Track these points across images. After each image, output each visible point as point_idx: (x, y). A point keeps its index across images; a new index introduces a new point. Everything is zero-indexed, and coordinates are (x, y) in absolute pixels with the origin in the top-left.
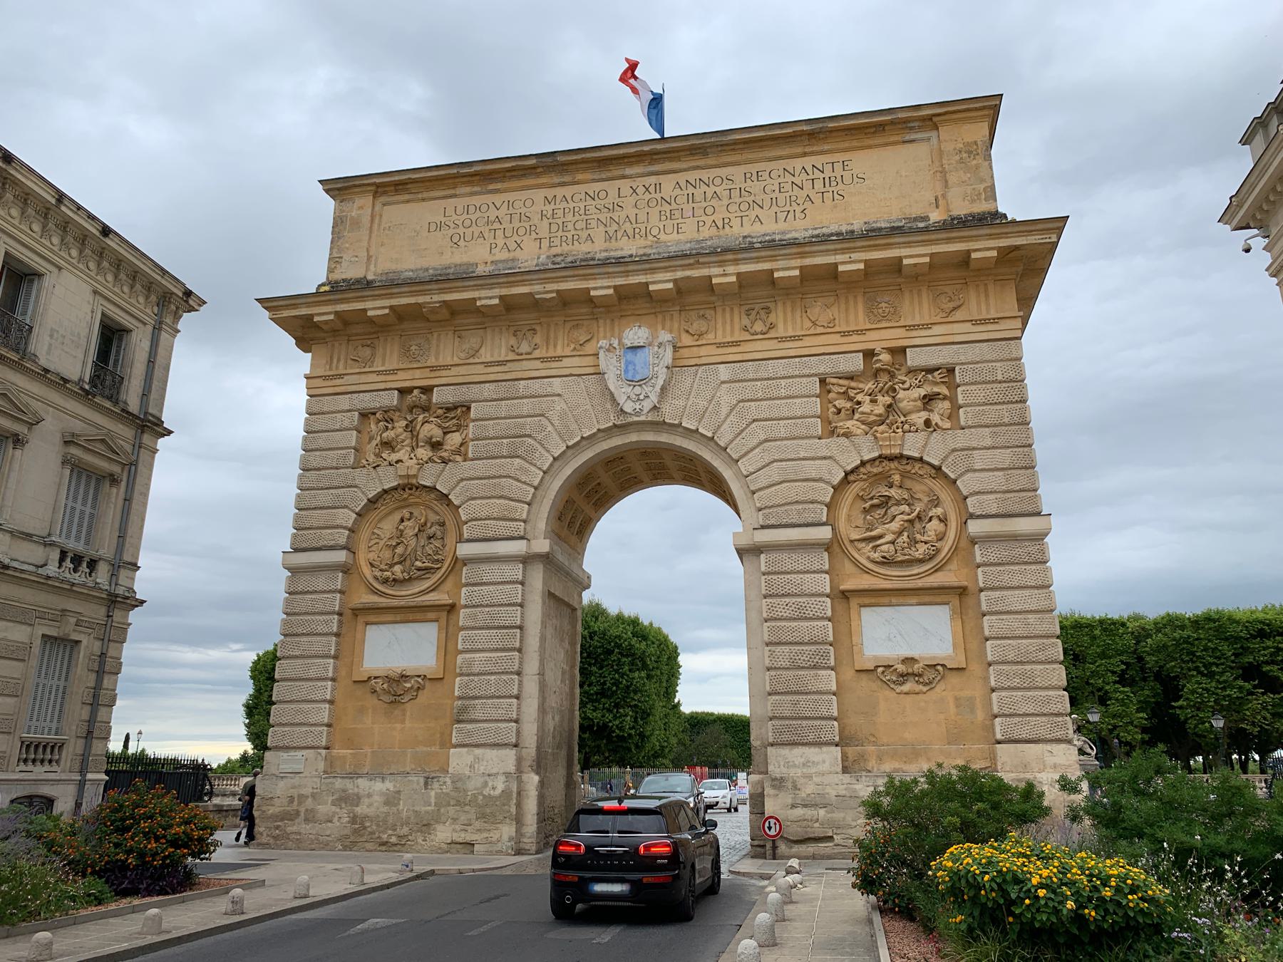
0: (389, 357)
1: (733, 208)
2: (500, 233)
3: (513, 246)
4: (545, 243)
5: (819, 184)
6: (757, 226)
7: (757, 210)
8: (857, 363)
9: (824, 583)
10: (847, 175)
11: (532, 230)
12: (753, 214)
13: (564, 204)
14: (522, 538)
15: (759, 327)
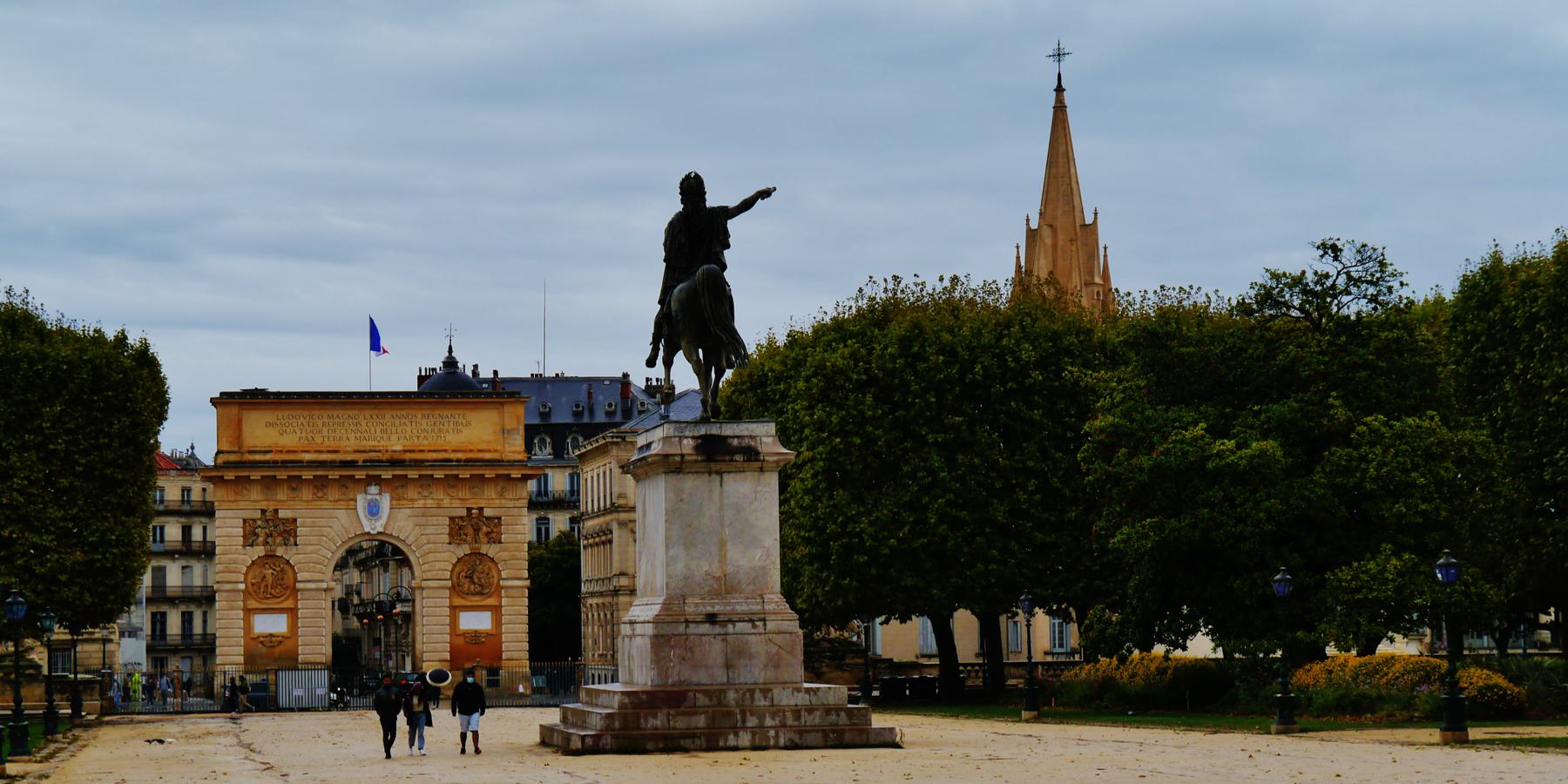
0: (255, 494)
1: (414, 431)
2: (304, 431)
3: (310, 439)
4: (326, 439)
5: (451, 424)
6: (425, 442)
7: (426, 434)
8: (464, 513)
9: (447, 602)
10: (464, 424)
11: (320, 431)
12: (423, 435)
13: (338, 420)
14: (322, 581)
15: (425, 493)
